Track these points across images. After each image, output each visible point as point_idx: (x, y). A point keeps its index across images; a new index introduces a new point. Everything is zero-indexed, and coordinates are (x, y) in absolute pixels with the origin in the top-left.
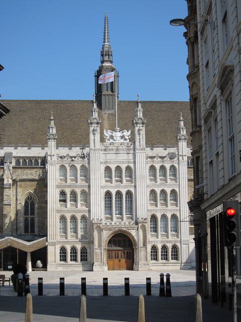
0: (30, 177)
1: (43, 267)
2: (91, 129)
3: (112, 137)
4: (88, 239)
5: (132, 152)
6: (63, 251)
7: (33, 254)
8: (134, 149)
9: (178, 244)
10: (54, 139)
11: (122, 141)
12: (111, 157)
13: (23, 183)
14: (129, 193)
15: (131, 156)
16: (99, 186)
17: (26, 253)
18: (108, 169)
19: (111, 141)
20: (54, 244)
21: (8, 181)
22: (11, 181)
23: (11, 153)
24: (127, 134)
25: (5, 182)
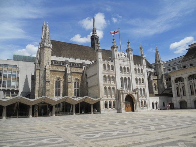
0: (77, 71)
1: (98, 111)
2: (115, 50)
3: (121, 55)
4: (118, 99)
5: (129, 62)
6: (106, 103)
7: (93, 105)
8: (130, 61)
9: (146, 100)
10: (101, 52)
11: (125, 57)
12: (122, 63)
13: (74, 74)
14: (129, 78)
15: (129, 63)
16: (119, 75)
17: (91, 105)
18: (121, 68)
19: (121, 56)
20: (103, 100)
21: (69, 72)
22: (70, 72)
23: (68, 61)
24: (126, 54)
25: (68, 72)
